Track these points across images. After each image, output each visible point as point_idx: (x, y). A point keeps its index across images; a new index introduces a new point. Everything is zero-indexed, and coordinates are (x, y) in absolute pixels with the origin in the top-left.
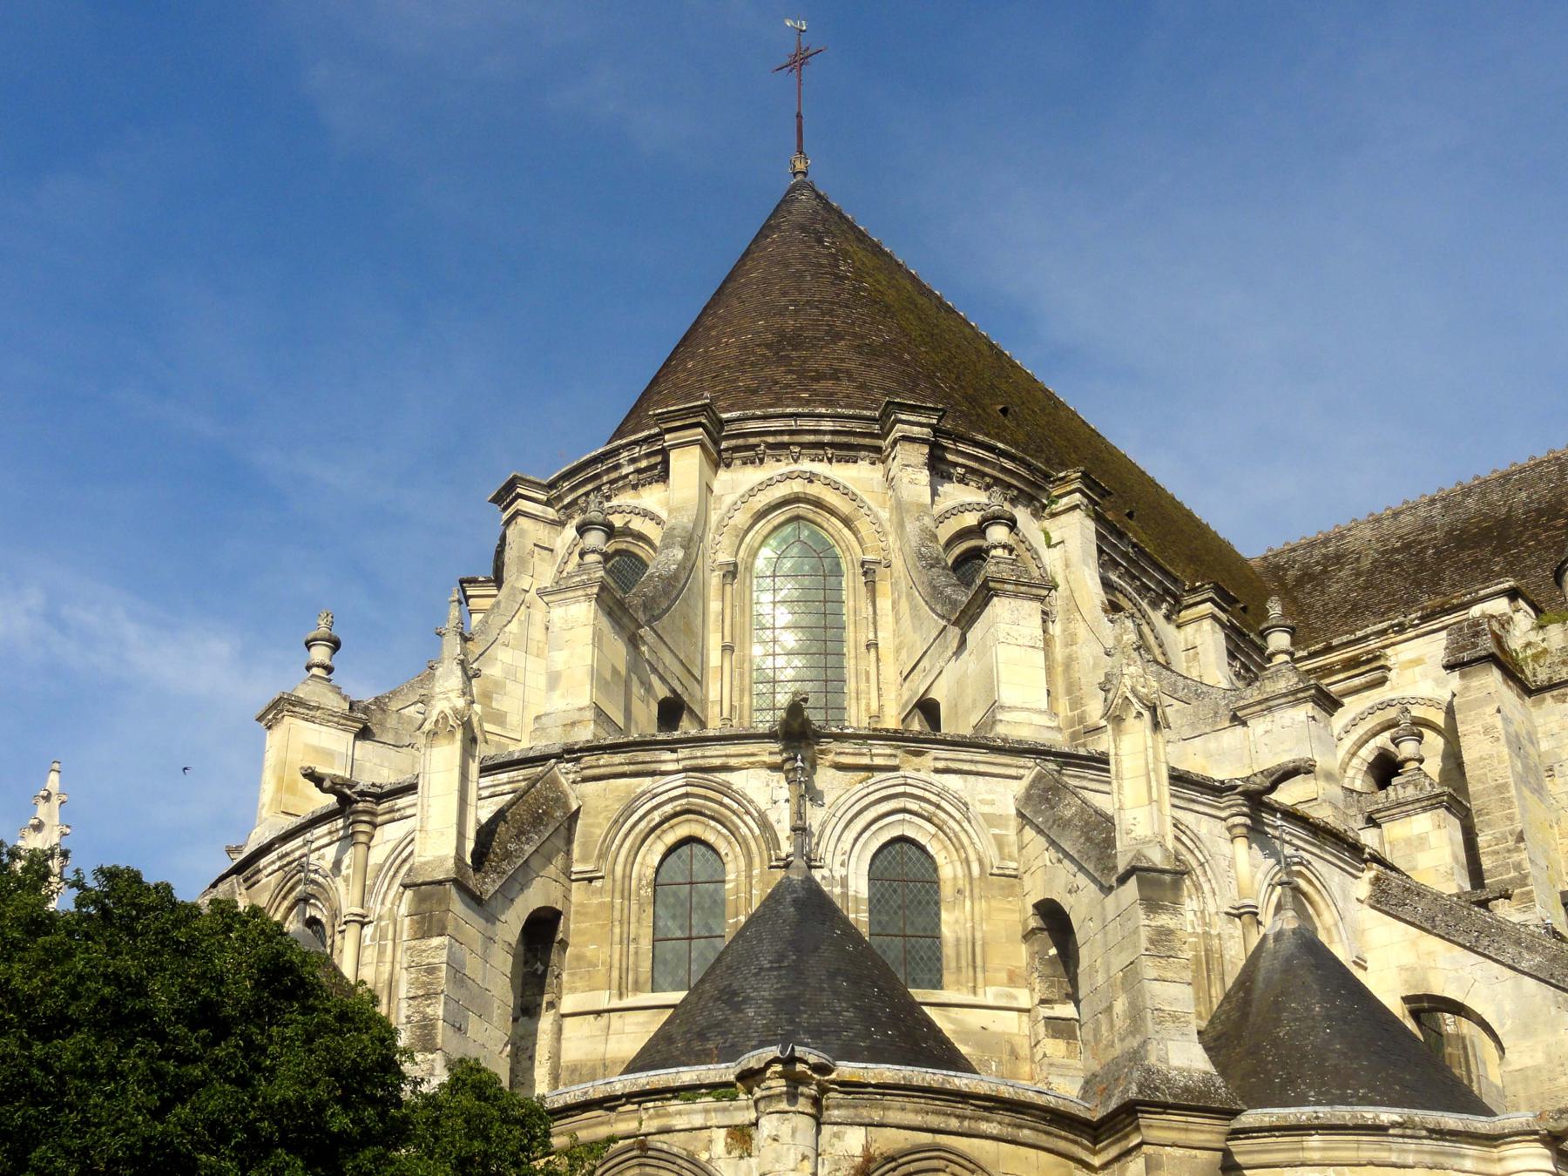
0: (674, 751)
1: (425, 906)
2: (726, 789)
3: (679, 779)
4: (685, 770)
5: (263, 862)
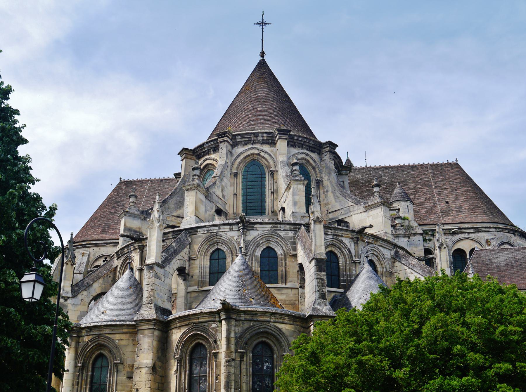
1: (320, 264)
2: (342, 242)
3: (331, 237)
4: (333, 235)
5: (199, 230)
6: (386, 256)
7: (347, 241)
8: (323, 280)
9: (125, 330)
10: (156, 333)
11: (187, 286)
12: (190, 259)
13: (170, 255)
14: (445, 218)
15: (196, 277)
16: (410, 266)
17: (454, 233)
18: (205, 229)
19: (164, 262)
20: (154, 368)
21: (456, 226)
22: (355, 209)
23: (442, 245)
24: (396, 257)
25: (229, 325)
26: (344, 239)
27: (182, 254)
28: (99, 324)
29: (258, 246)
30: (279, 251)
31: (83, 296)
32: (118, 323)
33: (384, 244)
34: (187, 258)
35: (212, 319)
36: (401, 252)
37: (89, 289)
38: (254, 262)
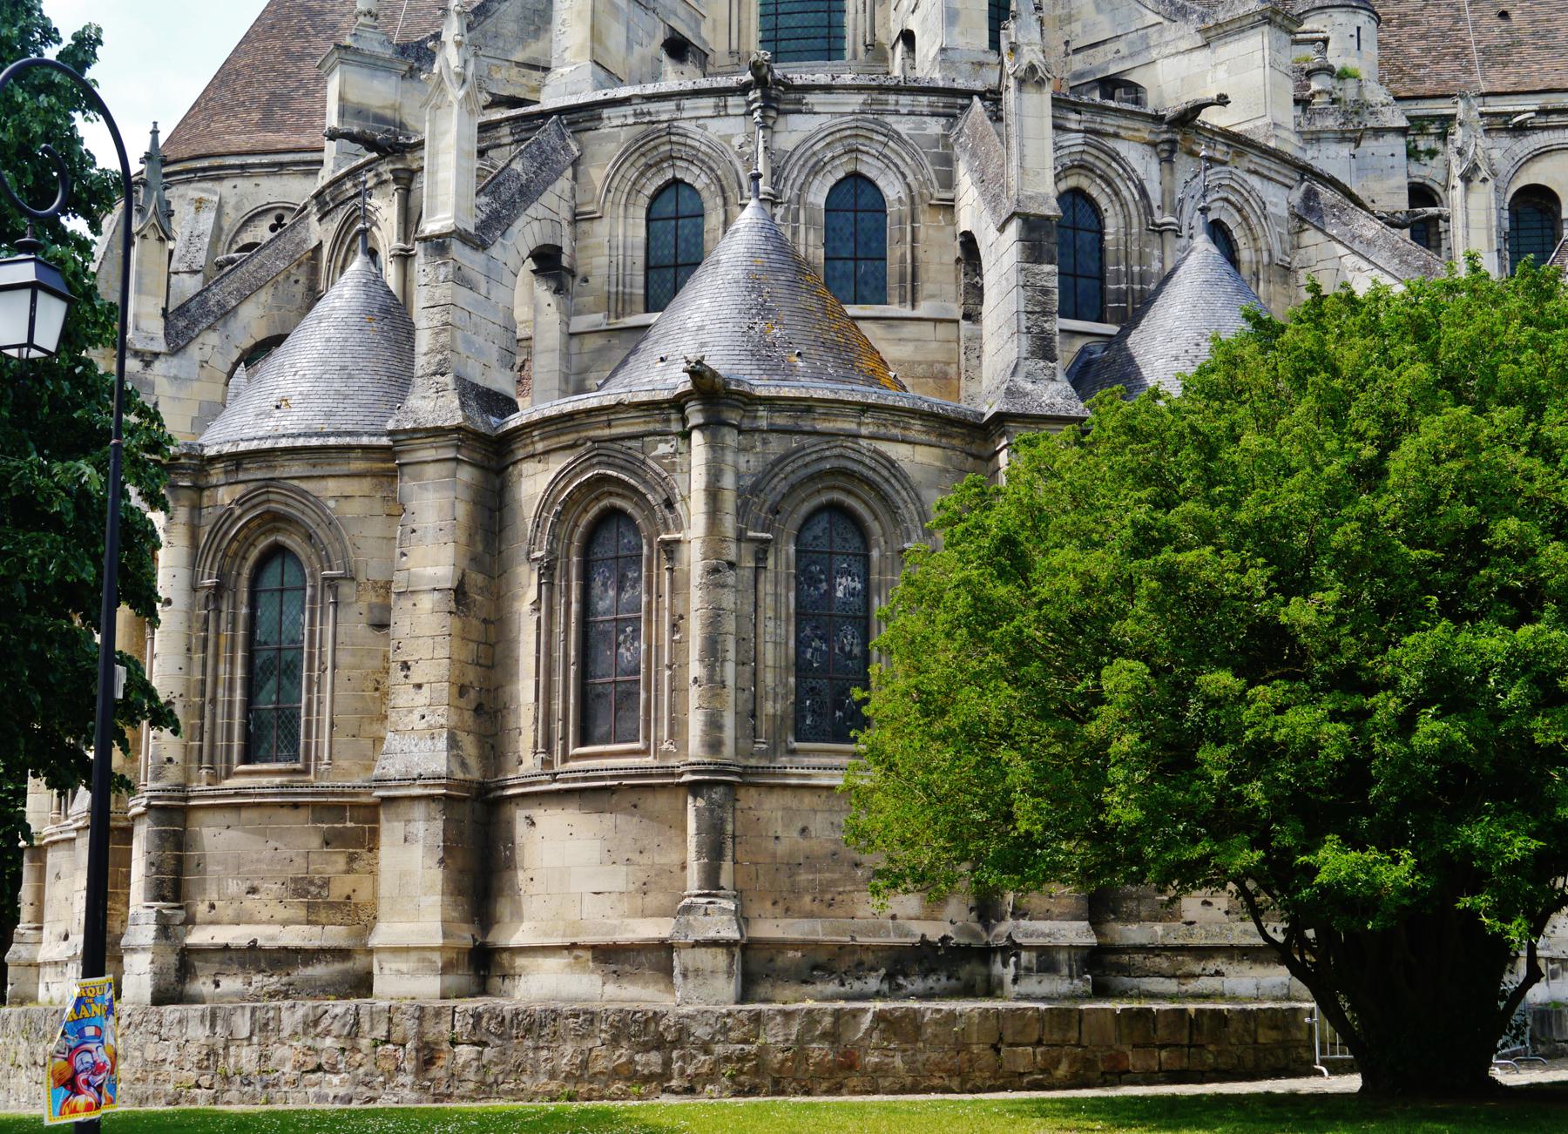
0: (1079, 113)
1: (1035, 236)
2: (1115, 156)
3: (1078, 138)
4: (1086, 131)
5: (606, 113)
6: (1270, 209)
7: (1137, 156)
8: (1045, 292)
9: (358, 465)
10: (466, 474)
11: (568, 314)
12: (577, 218)
13: (504, 205)
14: (1492, 73)
15: (598, 281)
16: (1356, 246)
17: (1521, 129)
18: (628, 110)
19: (484, 226)
20: (460, 593)
21: (1533, 103)
22: (1168, 36)
23: (1476, 168)
24: (1307, 214)
25: (714, 446)
26: (1122, 148)
27: (549, 198)
28: (268, 444)
29: (816, 170)
30: (892, 190)
31: (207, 349)
32: (332, 441)
33: (1265, 165)
34: (566, 214)
35: (659, 427)
36: (1327, 195)
37: (225, 325)
38: (802, 228)
